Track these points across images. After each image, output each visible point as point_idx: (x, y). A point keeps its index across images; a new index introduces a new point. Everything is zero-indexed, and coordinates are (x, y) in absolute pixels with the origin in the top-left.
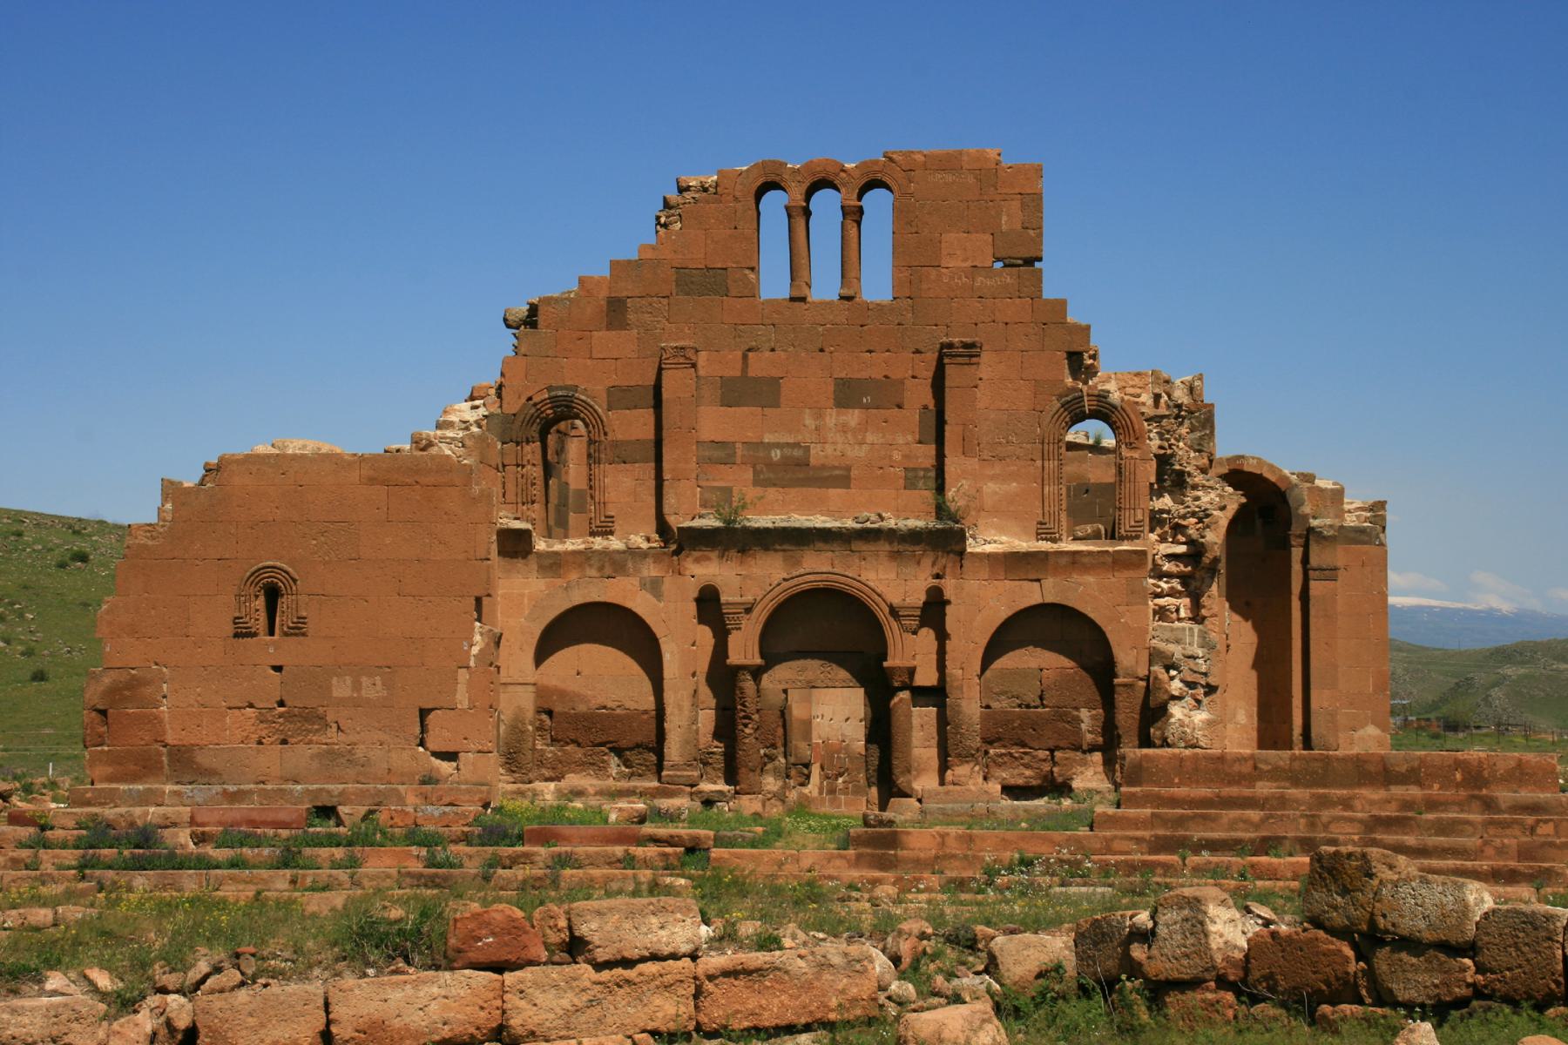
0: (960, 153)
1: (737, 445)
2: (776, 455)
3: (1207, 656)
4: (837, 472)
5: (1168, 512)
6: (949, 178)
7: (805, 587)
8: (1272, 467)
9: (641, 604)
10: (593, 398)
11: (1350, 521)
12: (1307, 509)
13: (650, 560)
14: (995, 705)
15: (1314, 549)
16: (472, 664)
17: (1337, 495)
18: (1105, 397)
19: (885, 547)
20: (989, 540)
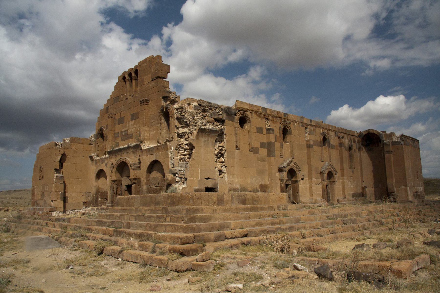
0: (147, 58)
1: (120, 133)
2: (124, 133)
3: (184, 170)
4: (131, 135)
5: (186, 133)
6: (145, 64)
7: (120, 162)
8: (376, 131)
9: (105, 169)
10: (104, 128)
11: (395, 140)
12: (384, 139)
13: (106, 159)
14: (152, 187)
15: (385, 147)
16: (54, 183)
17: (392, 134)
18: (167, 106)
19: (131, 150)
20: (146, 146)
